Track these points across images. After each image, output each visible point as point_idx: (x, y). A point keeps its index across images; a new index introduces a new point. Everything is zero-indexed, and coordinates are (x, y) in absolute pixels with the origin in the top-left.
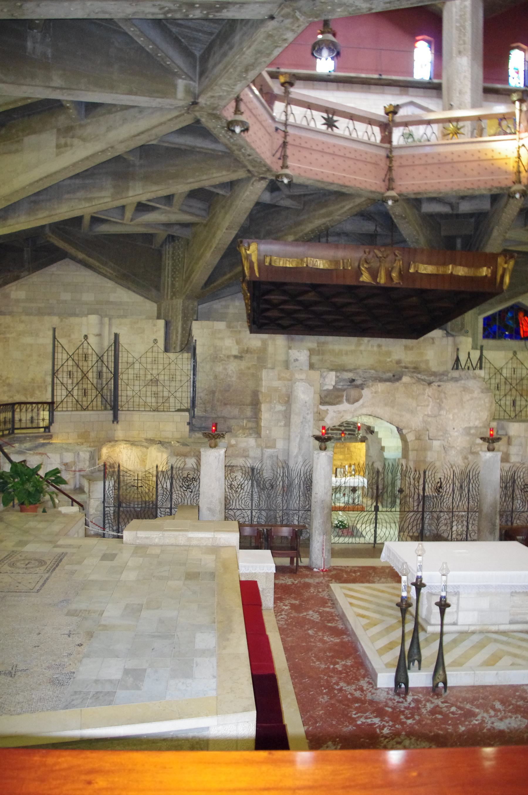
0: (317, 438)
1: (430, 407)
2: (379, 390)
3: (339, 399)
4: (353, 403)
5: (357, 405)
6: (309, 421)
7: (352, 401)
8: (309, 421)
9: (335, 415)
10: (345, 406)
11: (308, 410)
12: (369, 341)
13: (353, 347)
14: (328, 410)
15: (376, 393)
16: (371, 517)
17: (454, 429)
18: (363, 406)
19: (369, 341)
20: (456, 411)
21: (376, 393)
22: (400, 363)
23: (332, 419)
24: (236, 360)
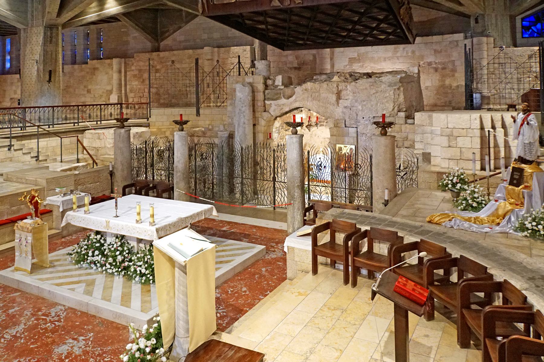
0: (176, 122)
1: (350, 100)
2: (309, 88)
3: (279, 96)
4: (288, 98)
5: (291, 100)
6: (244, 112)
7: (286, 96)
8: (244, 112)
9: (276, 107)
10: (283, 101)
11: (243, 104)
12: (404, 49)
13: (390, 54)
14: (271, 104)
15: (306, 90)
16: (270, 186)
17: (363, 118)
18: (295, 101)
19: (404, 49)
20: (365, 103)
21: (306, 90)
22: (431, 65)
23: (274, 110)
24: (296, 71)
